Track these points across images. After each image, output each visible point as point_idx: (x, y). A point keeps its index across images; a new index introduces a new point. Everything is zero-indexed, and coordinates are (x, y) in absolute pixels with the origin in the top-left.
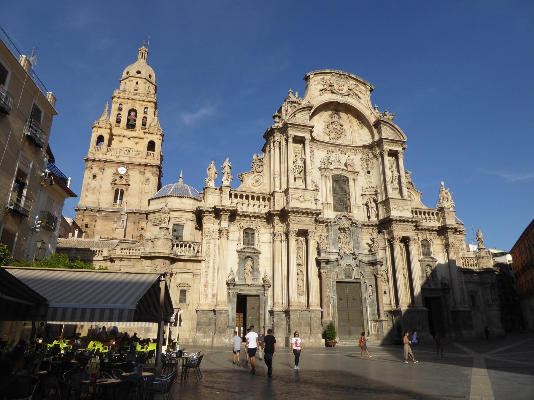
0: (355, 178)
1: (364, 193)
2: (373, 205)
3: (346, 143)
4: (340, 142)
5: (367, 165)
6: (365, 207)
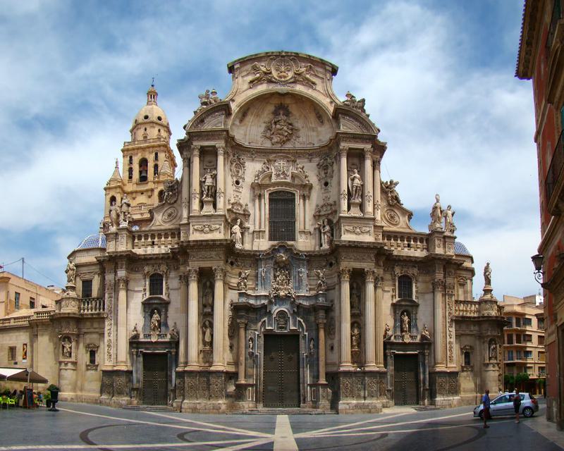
0: (306, 193)
1: (318, 214)
2: (327, 228)
3: (298, 146)
4: (289, 146)
5: (326, 173)
6: (317, 232)
